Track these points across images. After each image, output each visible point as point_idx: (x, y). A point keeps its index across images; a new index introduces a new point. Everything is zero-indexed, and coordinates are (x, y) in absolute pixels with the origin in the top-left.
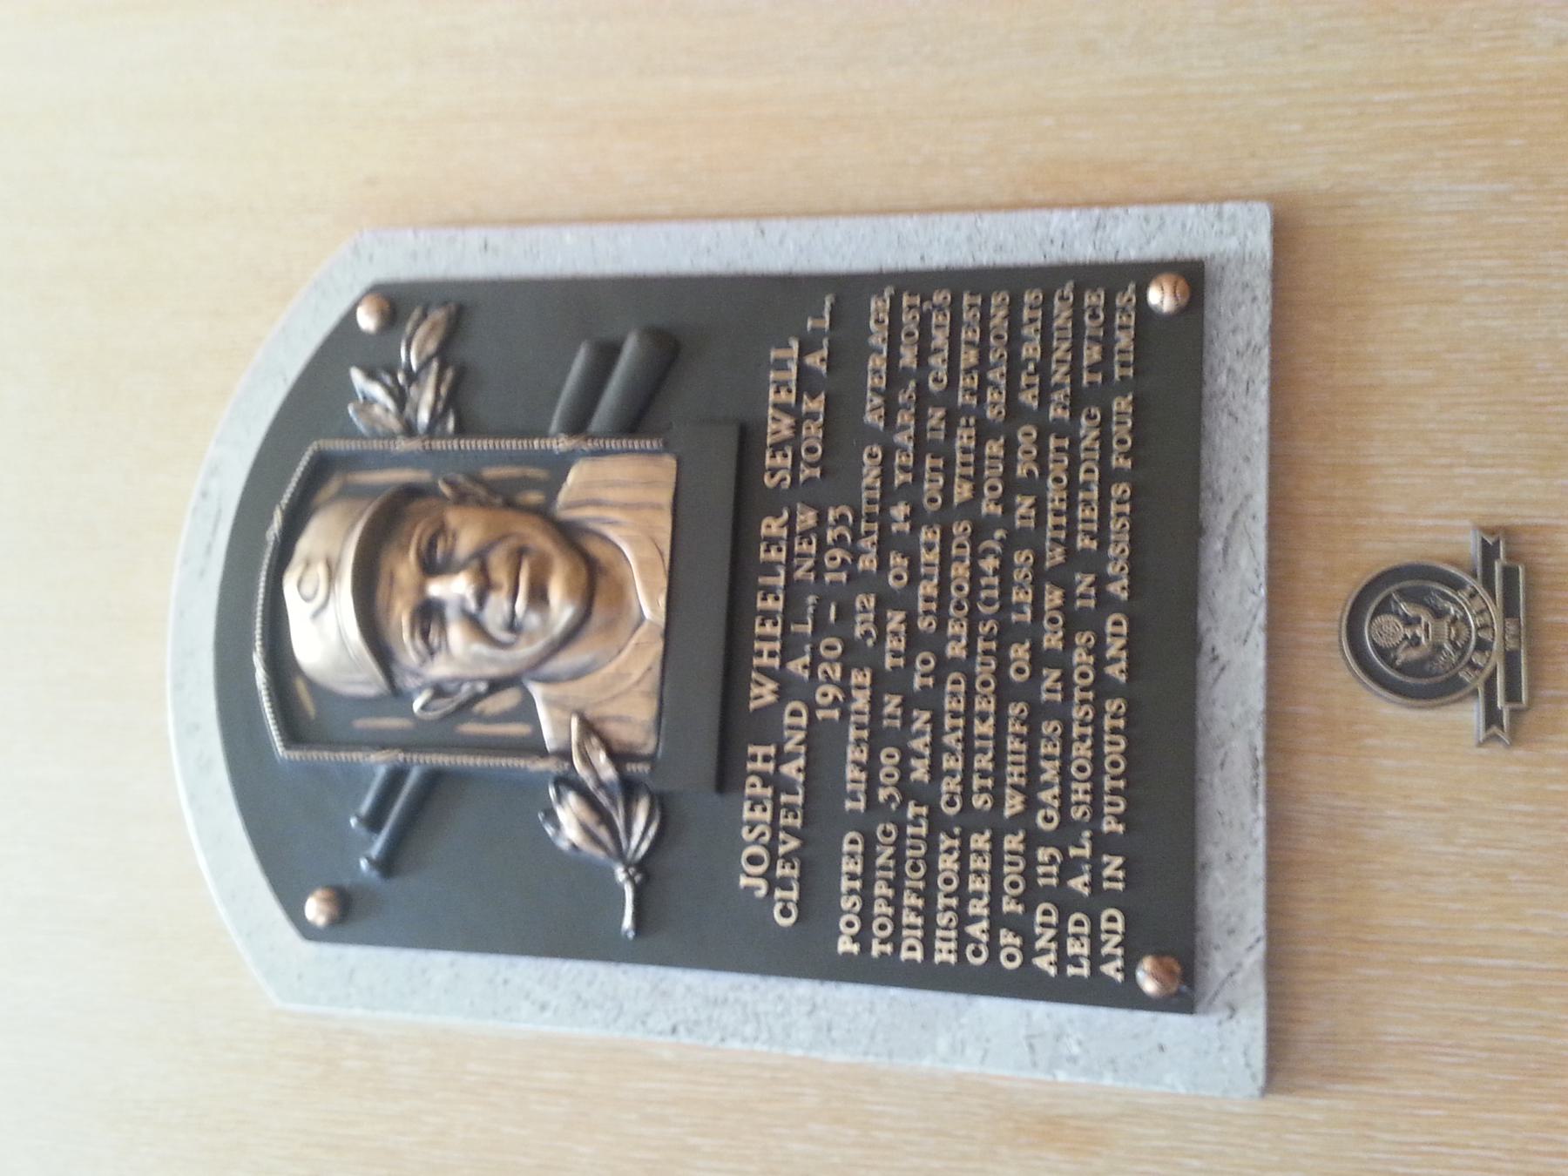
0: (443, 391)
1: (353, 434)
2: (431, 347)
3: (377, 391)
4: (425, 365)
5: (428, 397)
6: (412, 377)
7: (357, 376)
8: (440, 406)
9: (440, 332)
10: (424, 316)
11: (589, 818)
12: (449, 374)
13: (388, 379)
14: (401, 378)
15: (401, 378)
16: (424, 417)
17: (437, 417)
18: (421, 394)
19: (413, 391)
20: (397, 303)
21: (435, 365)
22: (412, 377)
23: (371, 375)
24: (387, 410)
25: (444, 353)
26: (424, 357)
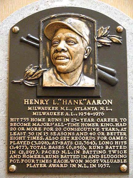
1: (98, 28)
2: (114, 41)
3: (106, 31)
8: (103, 43)
9: (117, 41)
10: (119, 38)
11: (31, 73)
14: (108, 36)
15: (108, 36)
16: (102, 40)
17: (101, 43)
21: (111, 42)
23: (108, 30)
24: (102, 34)
25: (113, 43)
26: (112, 40)
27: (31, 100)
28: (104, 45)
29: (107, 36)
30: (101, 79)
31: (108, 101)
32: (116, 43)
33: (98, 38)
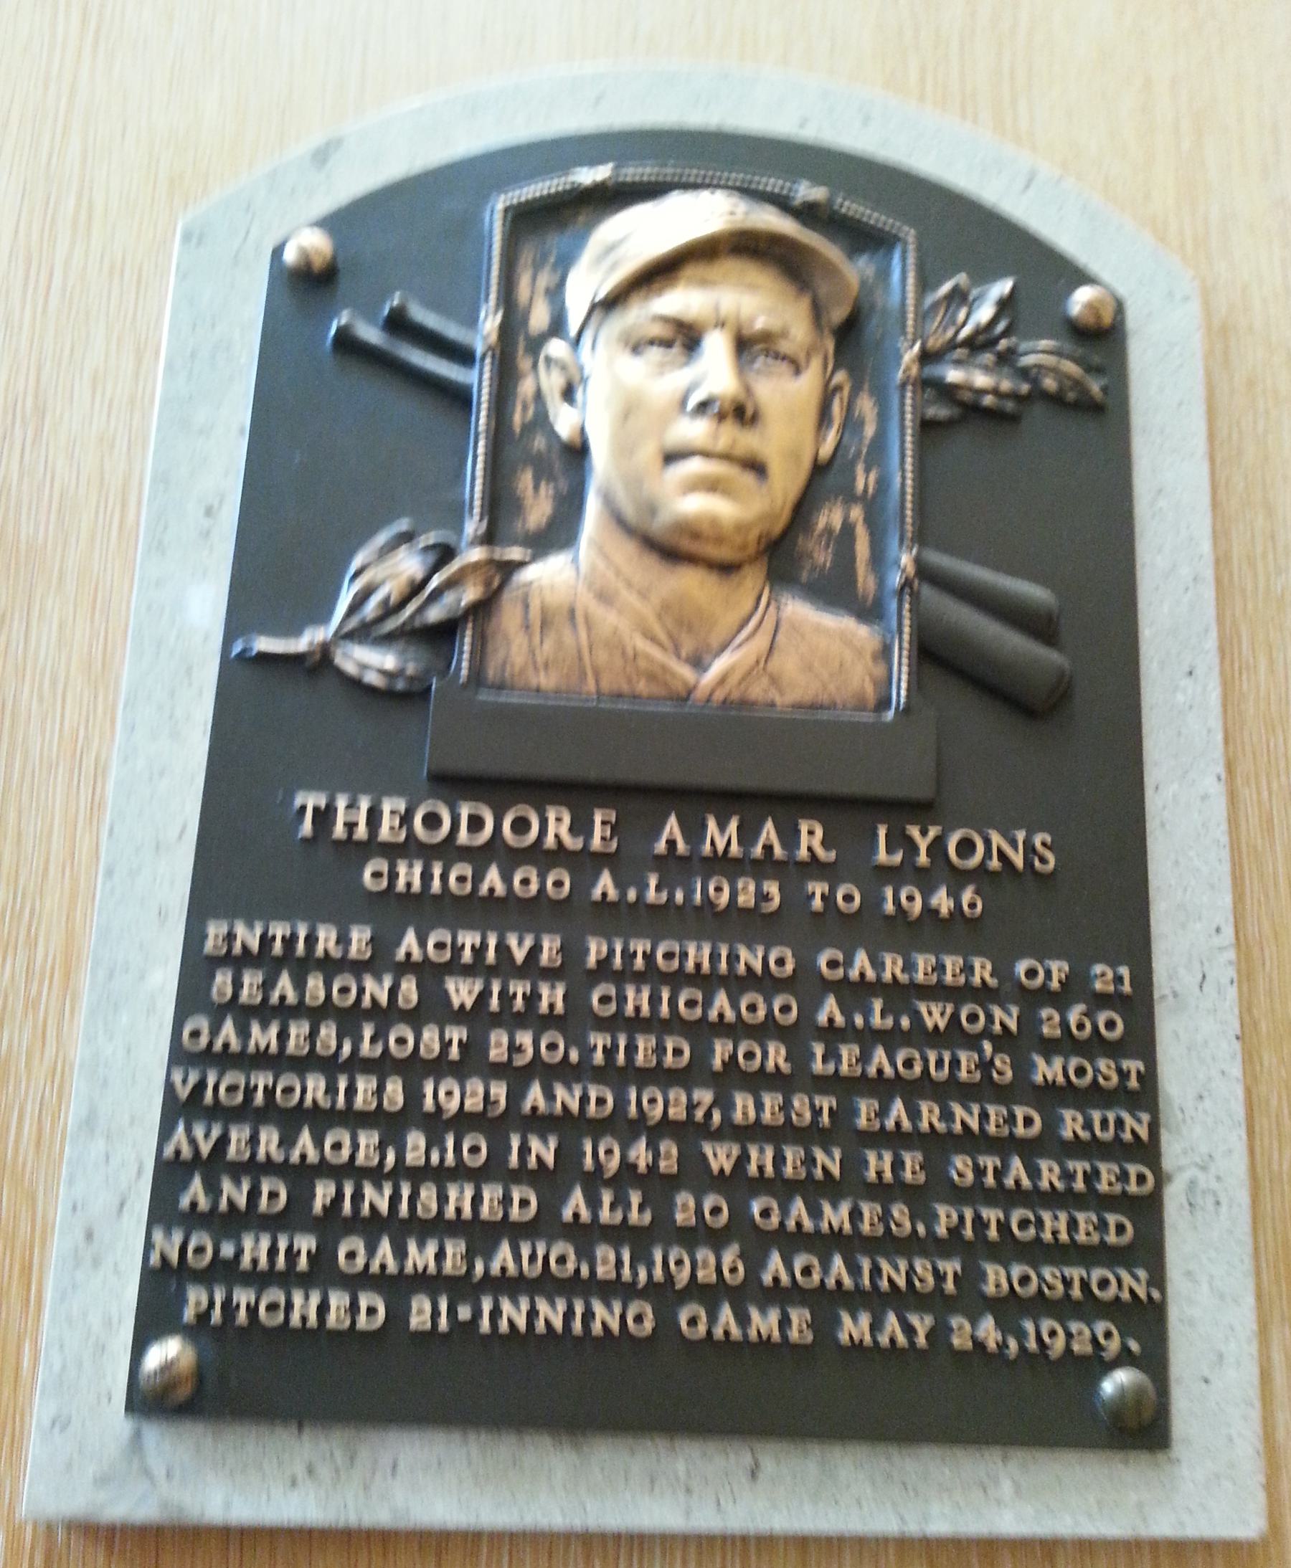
0: (988, 400)
2: (1049, 383)
4: (1024, 373)
5: (981, 380)
6: (1006, 359)
7: (1004, 287)
12: (1009, 406)
13: (1001, 327)
14: (1003, 344)
15: (1003, 344)
16: (953, 375)
17: (947, 392)
18: (986, 369)
19: (988, 358)
20: (1102, 339)
21: (1025, 388)
22: (1006, 359)
23: (1004, 305)
27: (387, 807)
28: (970, 409)
29: (995, 341)
30: (935, 655)
31: (996, 839)
32: (1056, 400)
33: (927, 357)
